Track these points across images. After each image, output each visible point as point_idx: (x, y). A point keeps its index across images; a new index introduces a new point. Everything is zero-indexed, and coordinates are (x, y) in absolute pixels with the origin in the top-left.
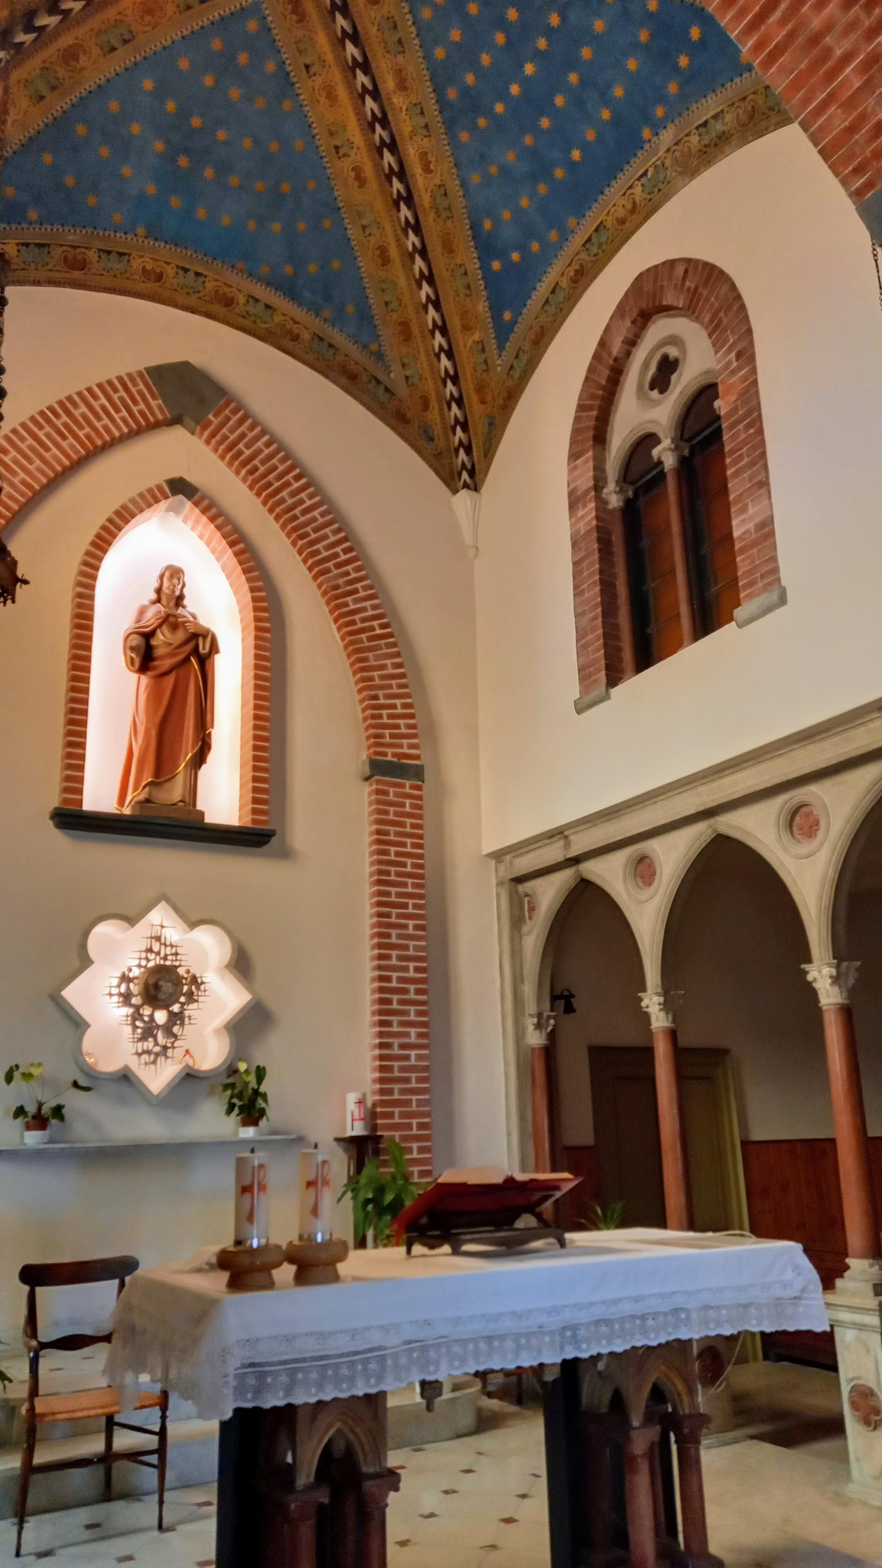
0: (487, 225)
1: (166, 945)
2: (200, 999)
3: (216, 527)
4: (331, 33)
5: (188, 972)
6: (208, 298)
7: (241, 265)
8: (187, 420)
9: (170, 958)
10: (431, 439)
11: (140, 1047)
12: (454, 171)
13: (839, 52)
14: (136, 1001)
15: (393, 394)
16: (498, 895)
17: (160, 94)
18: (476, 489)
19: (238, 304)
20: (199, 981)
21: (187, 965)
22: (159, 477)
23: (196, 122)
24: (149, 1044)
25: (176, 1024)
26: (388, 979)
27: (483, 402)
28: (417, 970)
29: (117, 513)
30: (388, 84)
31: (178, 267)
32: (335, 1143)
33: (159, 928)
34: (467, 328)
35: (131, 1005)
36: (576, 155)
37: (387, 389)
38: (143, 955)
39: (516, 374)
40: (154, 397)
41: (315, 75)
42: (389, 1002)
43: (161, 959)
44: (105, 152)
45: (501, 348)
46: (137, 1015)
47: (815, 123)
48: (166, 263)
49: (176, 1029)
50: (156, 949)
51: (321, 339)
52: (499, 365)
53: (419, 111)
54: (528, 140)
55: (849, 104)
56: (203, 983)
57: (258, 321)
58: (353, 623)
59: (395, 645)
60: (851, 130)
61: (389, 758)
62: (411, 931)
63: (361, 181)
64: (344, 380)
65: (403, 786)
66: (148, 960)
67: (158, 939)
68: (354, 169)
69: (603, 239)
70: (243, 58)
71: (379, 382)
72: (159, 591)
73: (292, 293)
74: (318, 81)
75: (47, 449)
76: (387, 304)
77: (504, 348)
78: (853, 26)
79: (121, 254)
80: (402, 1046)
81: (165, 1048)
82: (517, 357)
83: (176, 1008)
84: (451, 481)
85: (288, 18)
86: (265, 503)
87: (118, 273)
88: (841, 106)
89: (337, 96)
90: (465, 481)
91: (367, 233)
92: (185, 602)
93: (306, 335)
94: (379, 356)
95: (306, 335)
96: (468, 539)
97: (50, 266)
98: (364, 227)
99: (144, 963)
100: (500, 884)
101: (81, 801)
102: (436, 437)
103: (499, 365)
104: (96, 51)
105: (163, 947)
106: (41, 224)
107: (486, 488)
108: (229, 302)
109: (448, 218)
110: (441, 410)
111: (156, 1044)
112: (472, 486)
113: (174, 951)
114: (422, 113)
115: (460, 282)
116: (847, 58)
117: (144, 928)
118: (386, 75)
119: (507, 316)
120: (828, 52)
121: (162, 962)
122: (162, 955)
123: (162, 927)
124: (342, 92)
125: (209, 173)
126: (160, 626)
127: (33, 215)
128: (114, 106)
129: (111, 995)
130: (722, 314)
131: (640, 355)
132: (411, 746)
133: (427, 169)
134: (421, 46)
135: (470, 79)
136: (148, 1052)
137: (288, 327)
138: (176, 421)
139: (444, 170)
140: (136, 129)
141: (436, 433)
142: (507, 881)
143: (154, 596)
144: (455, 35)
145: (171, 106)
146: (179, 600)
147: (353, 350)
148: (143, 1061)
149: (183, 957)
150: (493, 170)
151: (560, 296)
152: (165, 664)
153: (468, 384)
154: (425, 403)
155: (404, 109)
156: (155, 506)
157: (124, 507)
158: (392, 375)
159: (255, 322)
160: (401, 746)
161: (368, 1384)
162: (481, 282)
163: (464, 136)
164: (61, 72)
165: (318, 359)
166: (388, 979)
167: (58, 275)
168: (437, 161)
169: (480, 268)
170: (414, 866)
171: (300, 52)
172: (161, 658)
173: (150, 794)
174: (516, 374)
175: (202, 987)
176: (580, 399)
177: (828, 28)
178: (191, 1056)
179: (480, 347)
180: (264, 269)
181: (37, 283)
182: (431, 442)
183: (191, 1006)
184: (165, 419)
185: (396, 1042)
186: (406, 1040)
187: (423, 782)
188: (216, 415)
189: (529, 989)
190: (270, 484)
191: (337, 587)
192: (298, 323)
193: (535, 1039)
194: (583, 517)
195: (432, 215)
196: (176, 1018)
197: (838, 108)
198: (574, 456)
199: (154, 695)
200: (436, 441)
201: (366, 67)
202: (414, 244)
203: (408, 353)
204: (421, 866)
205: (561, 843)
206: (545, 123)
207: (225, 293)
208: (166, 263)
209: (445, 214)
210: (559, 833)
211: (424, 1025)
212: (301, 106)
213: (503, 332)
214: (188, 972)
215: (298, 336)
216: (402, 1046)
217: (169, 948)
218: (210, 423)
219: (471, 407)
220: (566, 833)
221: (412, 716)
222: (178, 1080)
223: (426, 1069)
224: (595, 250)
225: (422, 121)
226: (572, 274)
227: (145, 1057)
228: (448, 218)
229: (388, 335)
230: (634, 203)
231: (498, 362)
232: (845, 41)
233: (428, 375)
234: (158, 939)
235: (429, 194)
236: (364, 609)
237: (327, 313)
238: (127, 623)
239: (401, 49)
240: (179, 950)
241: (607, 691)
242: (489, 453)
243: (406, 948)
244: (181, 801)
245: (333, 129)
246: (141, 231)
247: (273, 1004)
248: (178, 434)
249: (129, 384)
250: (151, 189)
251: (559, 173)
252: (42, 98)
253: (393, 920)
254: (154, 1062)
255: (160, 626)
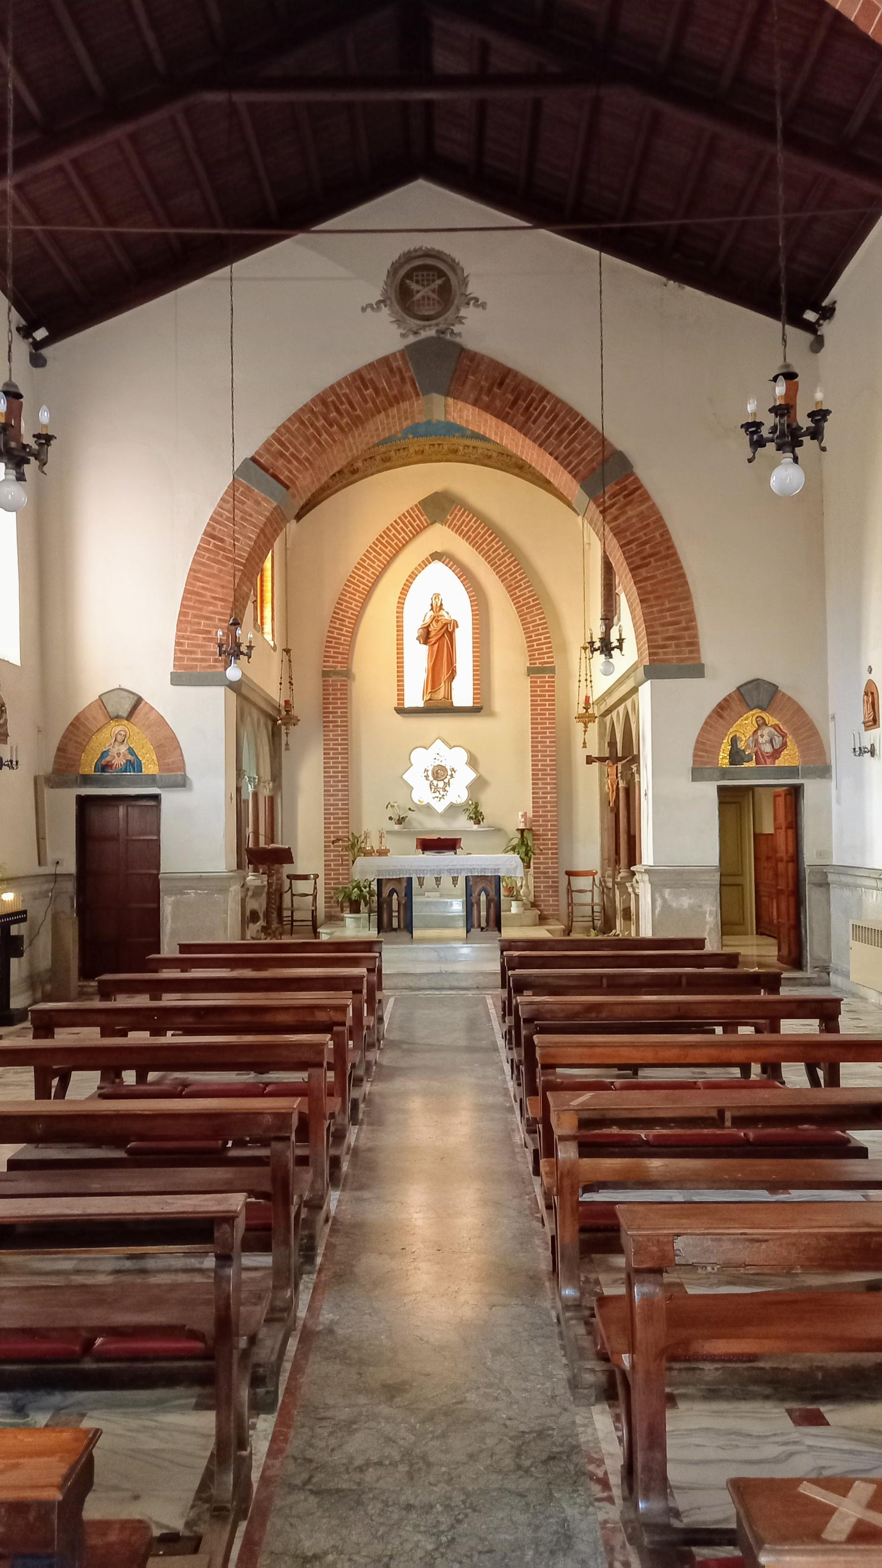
7: (457, 434)
14: (431, 778)
24: (437, 794)
40: (422, 516)
51: (503, 454)
59: (541, 608)
64: (517, 471)
72: (432, 605)
75: (380, 555)
79: (404, 449)
92: (444, 607)
93: (495, 455)
95: (495, 455)
108: (455, 451)
132: (548, 658)
138: (433, 523)
152: (433, 640)
181: (372, 474)
199: (430, 655)
211: (555, 784)
246: (410, 436)
248: (438, 527)
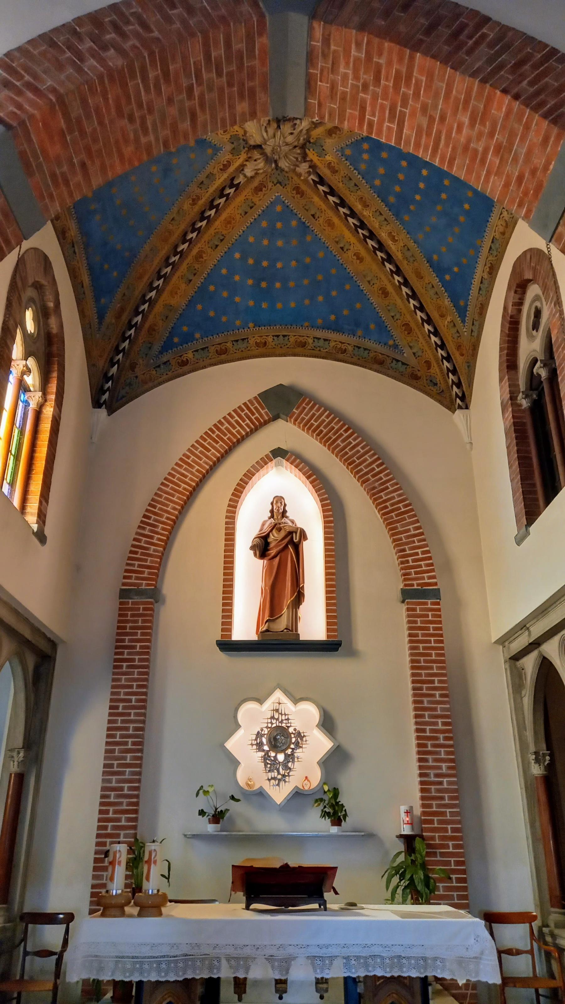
0: (435, 257)
1: (282, 714)
2: (304, 746)
3: (299, 470)
4: (319, 195)
5: (295, 730)
6: (291, 346)
7: (306, 324)
8: (281, 415)
9: (284, 722)
10: (436, 384)
11: (270, 775)
12: (408, 236)
13: (480, 149)
14: (266, 748)
15: (408, 365)
16: (506, 669)
17: (244, 258)
18: (467, 408)
19: (309, 343)
20: (302, 735)
21: (296, 725)
22: (267, 451)
23: (265, 264)
24: (275, 774)
25: (290, 761)
26: (424, 731)
27: (462, 355)
28: (444, 724)
29: (245, 475)
30: (358, 207)
31: (273, 336)
32: (397, 839)
33: (278, 704)
34: (442, 316)
35: (263, 751)
36: (467, 206)
37: (403, 364)
38: (269, 721)
39: (475, 334)
40: (263, 409)
41: (318, 217)
42: (425, 746)
43: (279, 722)
44: (225, 294)
45: (463, 321)
46: (266, 757)
47: (488, 186)
48: (267, 336)
49: (290, 765)
50: (276, 717)
51: (359, 348)
52: (465, 331)
53: (379, 213)
54: (439, 208)
55: (498, 173)
56: (304, 736)
57: (322, 349)
58: (386, 507)
59: (415, 516)
60: (507, 185)
61: (415, 587)
62: (438, 698)
63: (360, 259)
64: (376, 366)
65: (426, 604)
66: (272, 724)
67: (277, 710)
68: (354, 255)
69: (497, 245)
70: (279, 225)
71: (398, 361)
72: (272, 511)
73: (336, 328)
74: (321, 220)
75: (209, 450)
76: (393, 317)
77: (465, 321)
78: (480, 135)
79: (243, 340)
80: (437, 775)
81: (284, 776)
82: (473, 324)
83: (289, 751)
84: (452, 408)
85: (296, 197)
86: (329, 449)
87: (243, 349)
88: (495, 175)
89: (334, 223)
90: (459, 404)
91: (372, 284)
92: (288, 514)
93: (350, 348)
94: (396, 346)
95: (350, 348)
96: (466, 440)
97: (210, 357)
98: (369, 282)
99: (270, 725)
100: (505, 662)
101: (231, 635)
102: (438, 382)
103: (465, 331)
104: (209, 250)
105: (280, 715)
106: (202, 339)
107: (472, 406)
108: (303, 345)
109: (414, 261)
110: (439, 366)
111: (279, 773)
112: (464, 407)
113: (286, 718)
114: (381, 214)
115: (432, 292)
116: (486, 150)
117: (269, 704)
118: (356, 203)
119: (462, 303)
120: (476, 151)
121: (280, 725)
122: (280, 720)
123: (280, 704)
124: (336, 220)
125: (278, 285)
126: (271, 531)
127: (197, 335)
128: (224, 271)
129: (252, 745)
130: (546, 280)
131: (525, 309)
132: (429, 578)
133: (394, 240)
134: (367, 183)
135: (397, 188)
136: (274, 778)
137: (339, 347)
138: (275, 418)
139: (403, 237)
140: (237, 278)
141: (438, 380)
142: (508, 660)
143: (269, 515)
144: (381, 171)
145: (251, 261)
146: (284, 514)
147: (379, 348)
148: (272, 784)
149: (292, 721)
150: (427, 229)
151: (486, 282)
152: (273, 552)
153: (451, 347)
154: (428, 364)
155: (371, 215)
156: (265, 466)
157: (249, 471)
158: (405, 355)
159: (320, 350)
160: (423, 578)
161: (177, 974)
162: (443, 289)
163: (406, 218)
164: (197, 266)
165: (359, 359)
166: (424, 731)
167: (214, 360)
168: (398, 234)
169: (440, 281)
170: (437, 655)
171: (307, 210)
172: (272, 549)
173: (269, 626)
174: (475, 334)
175: (304, 739)
176: (500, 345)
177: (469, 141)
178: (308, 781)
179: (452, 324)
180: (320, 321)
181: (204, 367)
182: (435, 387)
183: (298, 751)
184: (269, 419)
185: (432, 772)
186: (440, 771)
187: (440, 600)
188: (297, 409)
189: (529, 734)
190: (330, 438)
191: (374, 488)
192: (344, 343)
193: (537, 770)
194: (507, 417)
195: (405, 262)
196: (290, 758)
197: (495, 176)
198: (501, 380)
199: (268, 570)
200: (439, 385)
201: (343, 203)
202: (398, 281)
203: (412, 339)
204: (443, 655)
205: (527, 633)
206: (444, 196)
207: (301, 341)
208: (267, 336)
209: (411, 259)
210: (523, 626)
211: (452, 761)
212: (316, 235)
213: (462, 312)
214: (295, 730)
215: (345, 350)
216: (437, 775)
217: (284, 716)
218: (294, 413)
219: (456, 360)
220: (528, 626)
221: (430, 558)
222: (291, 795)
223: (456, 791)
224: (495, 253)
225: (382, 218)
226: (488, 270)
227: (272, 781)
228: (414, 261)
229: (398, 334)
230: (506, 221)
231: (464, 330)
232: (480, 143)
233: (426, 348)
234: (277, 710)
235: (400, 252)
236: (393, 498)
237: (359, 333)
238: (255, 532)
239: (358, 188)
240: (290, 717)
241: (526, 529)
242: (470, 385)
243: (435, 709)
244: (286, 629)
245: (337, 240)
246: (251, 325)
247: (349, 747)
248: (280, 423)
249: (250, 405)
250: (251, 303)
251: (462, 219)
252: (190, 281)
253: (425, 691)
254: (278, 785)
255: (271, 531)
